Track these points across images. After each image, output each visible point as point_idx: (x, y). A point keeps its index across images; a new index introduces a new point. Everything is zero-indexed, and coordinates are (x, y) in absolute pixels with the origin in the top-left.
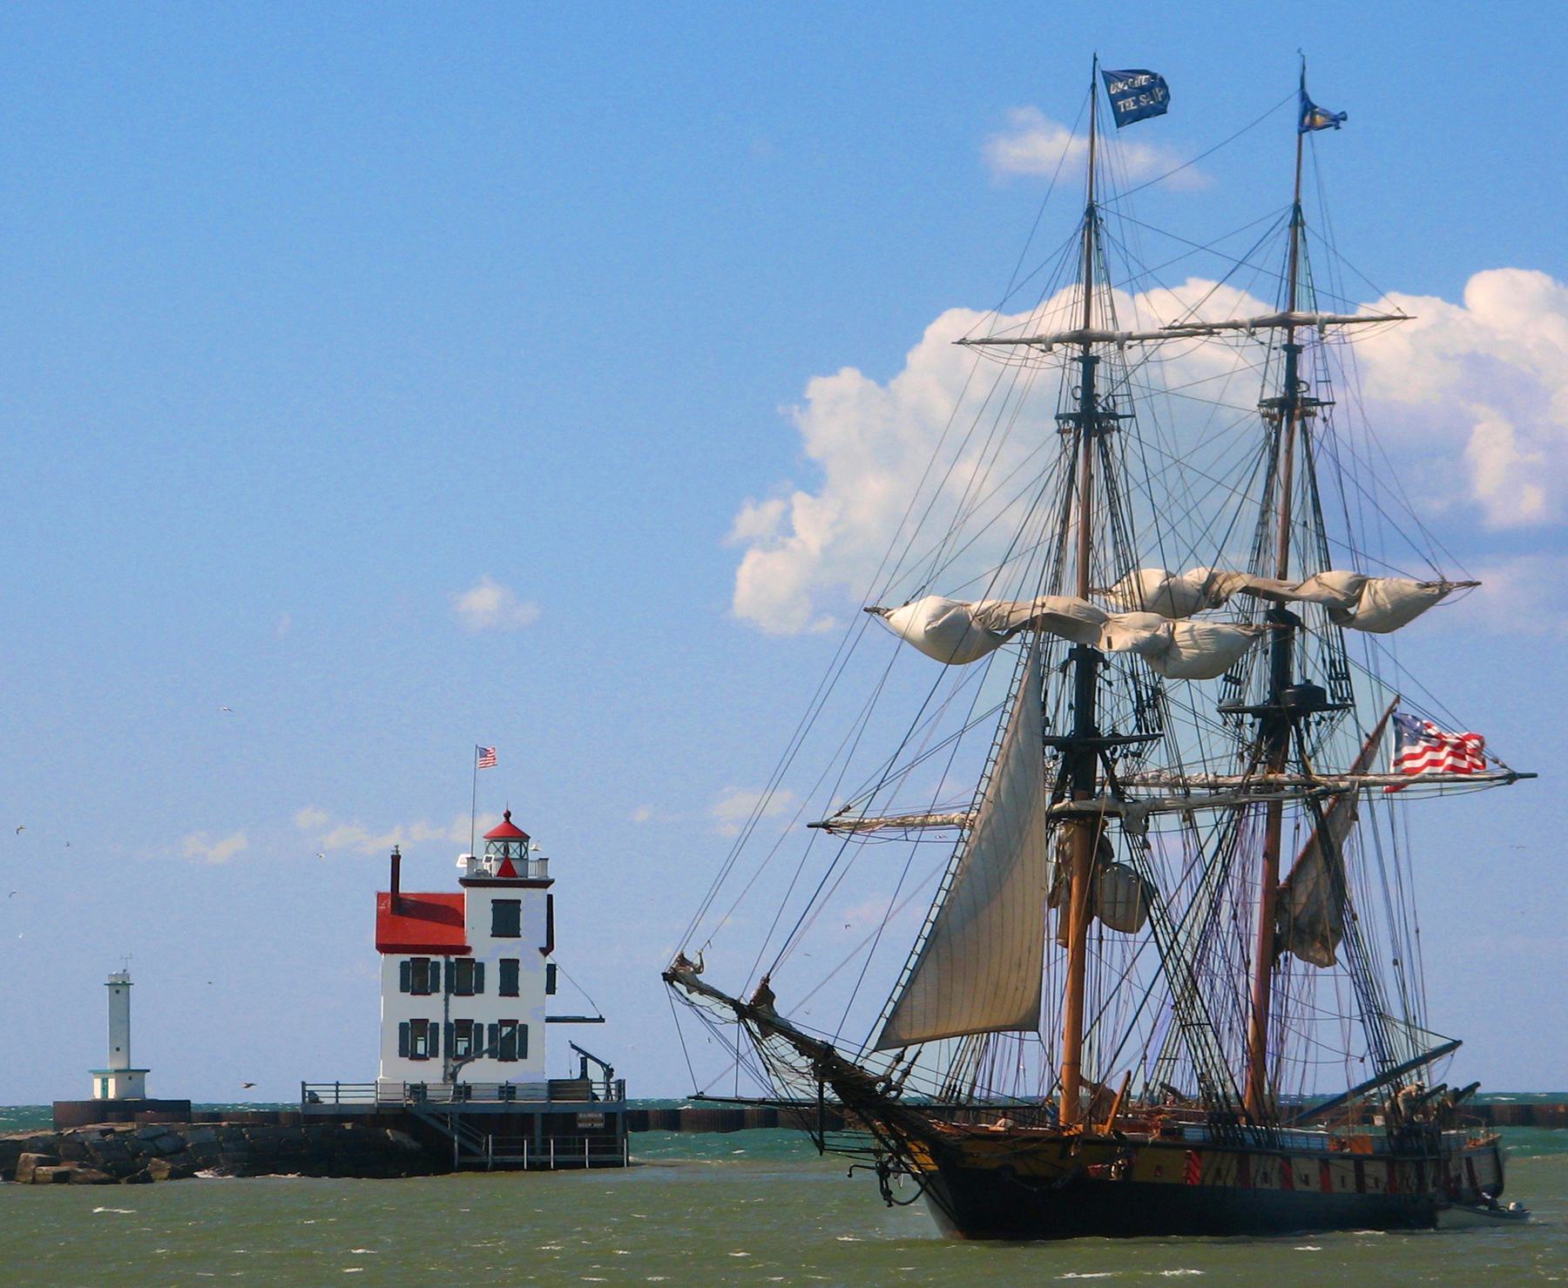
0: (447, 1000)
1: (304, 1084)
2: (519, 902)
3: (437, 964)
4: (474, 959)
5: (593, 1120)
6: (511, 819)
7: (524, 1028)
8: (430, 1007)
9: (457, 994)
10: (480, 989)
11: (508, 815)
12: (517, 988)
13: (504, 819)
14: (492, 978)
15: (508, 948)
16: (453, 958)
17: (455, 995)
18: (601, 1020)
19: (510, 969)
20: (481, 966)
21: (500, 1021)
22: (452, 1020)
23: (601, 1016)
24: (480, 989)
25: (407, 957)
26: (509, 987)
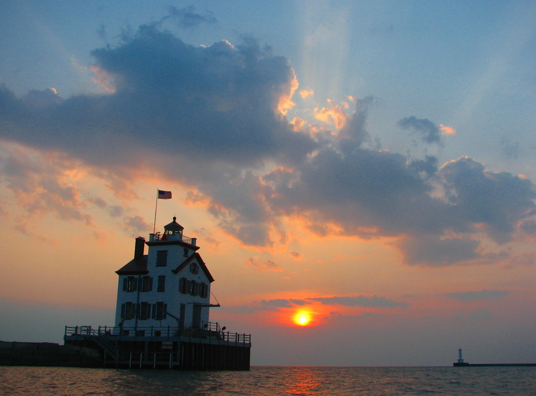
0: (139, 294)
1: (66, 326)
2: (167, 251)
3: (136, 278)
4: (149, 276)
5: (168, 345)
6: (177, 221)
7: (166, 305)
8: (132, 297)
9: (144, 291)
10: (151, 289)
11: (175, 218)
12: (164, 288)
13: (173, 220)
14: (155, 284)
15: (161, 271)
16: (142, 276)
17: (142, 292)
18: (218, 305)
19: (162, 279)
20: (152, 279)
21: (157, 302)
22: (140, 303)
23: (218, 304)
24: (151, 289)
25: (126, 277)
26: (161, 289)
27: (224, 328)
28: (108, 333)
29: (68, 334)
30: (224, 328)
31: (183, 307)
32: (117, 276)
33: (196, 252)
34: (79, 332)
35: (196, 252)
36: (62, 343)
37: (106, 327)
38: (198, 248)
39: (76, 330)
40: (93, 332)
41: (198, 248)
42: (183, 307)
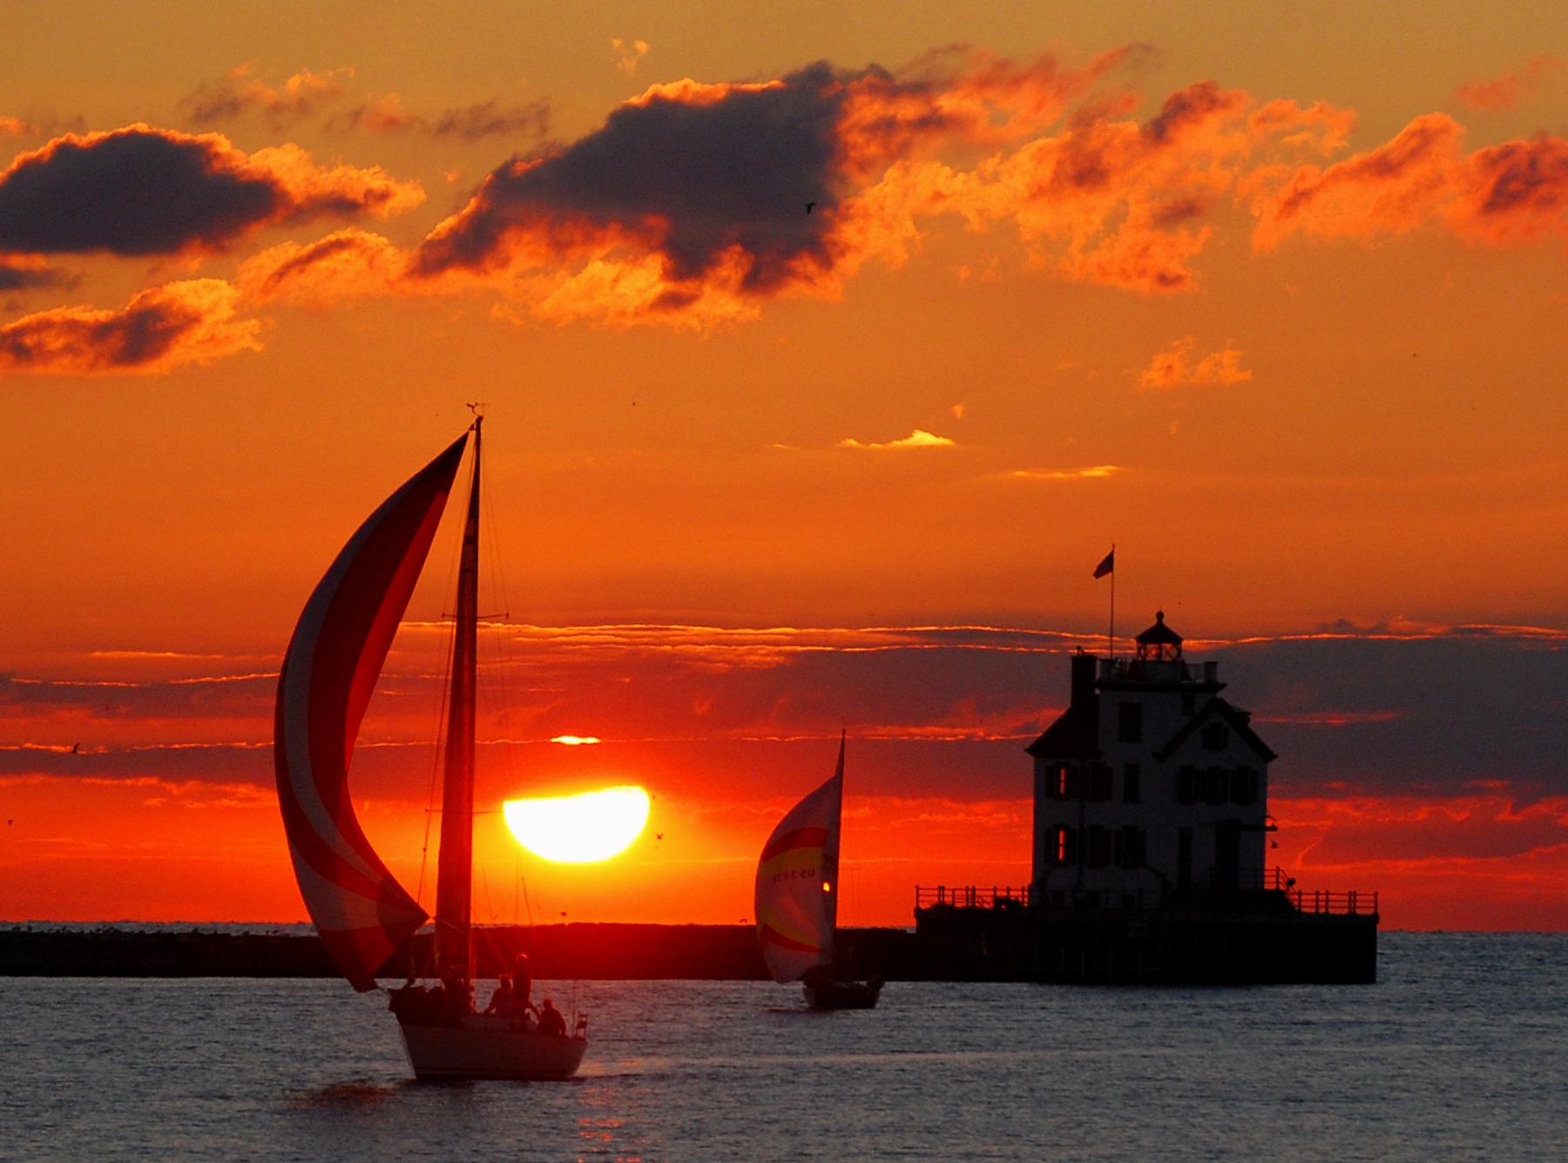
1: (918, 888)
6: (1164, 620)
11: (1160, 615)
19: (1132, 772)
26: (1132, 795)
27: (1291, 882)
28: (1013, 905)
29: (923, 906)
30: (1291, 882)
31: (1185, 838)
32: (1031, 759)
33: (1220, 695)
34: (948, 900)
35: (1220, 695)
36: (909, 924)
37: (1008, 890)
38: (1223, 686)
39: (941, 895)
40: (980, 900)
41: (1223, 686)
42: (1185, 838)
